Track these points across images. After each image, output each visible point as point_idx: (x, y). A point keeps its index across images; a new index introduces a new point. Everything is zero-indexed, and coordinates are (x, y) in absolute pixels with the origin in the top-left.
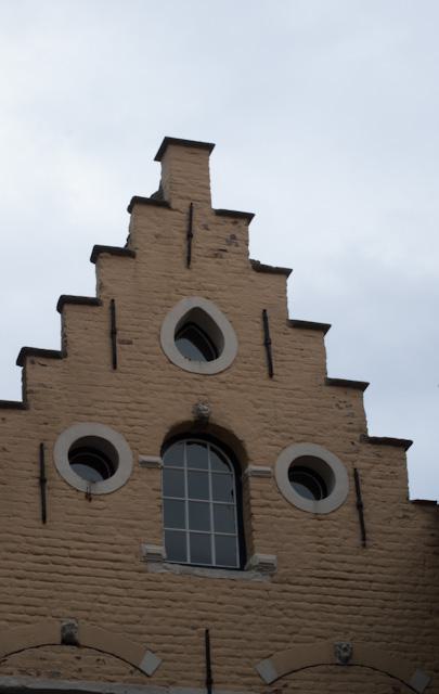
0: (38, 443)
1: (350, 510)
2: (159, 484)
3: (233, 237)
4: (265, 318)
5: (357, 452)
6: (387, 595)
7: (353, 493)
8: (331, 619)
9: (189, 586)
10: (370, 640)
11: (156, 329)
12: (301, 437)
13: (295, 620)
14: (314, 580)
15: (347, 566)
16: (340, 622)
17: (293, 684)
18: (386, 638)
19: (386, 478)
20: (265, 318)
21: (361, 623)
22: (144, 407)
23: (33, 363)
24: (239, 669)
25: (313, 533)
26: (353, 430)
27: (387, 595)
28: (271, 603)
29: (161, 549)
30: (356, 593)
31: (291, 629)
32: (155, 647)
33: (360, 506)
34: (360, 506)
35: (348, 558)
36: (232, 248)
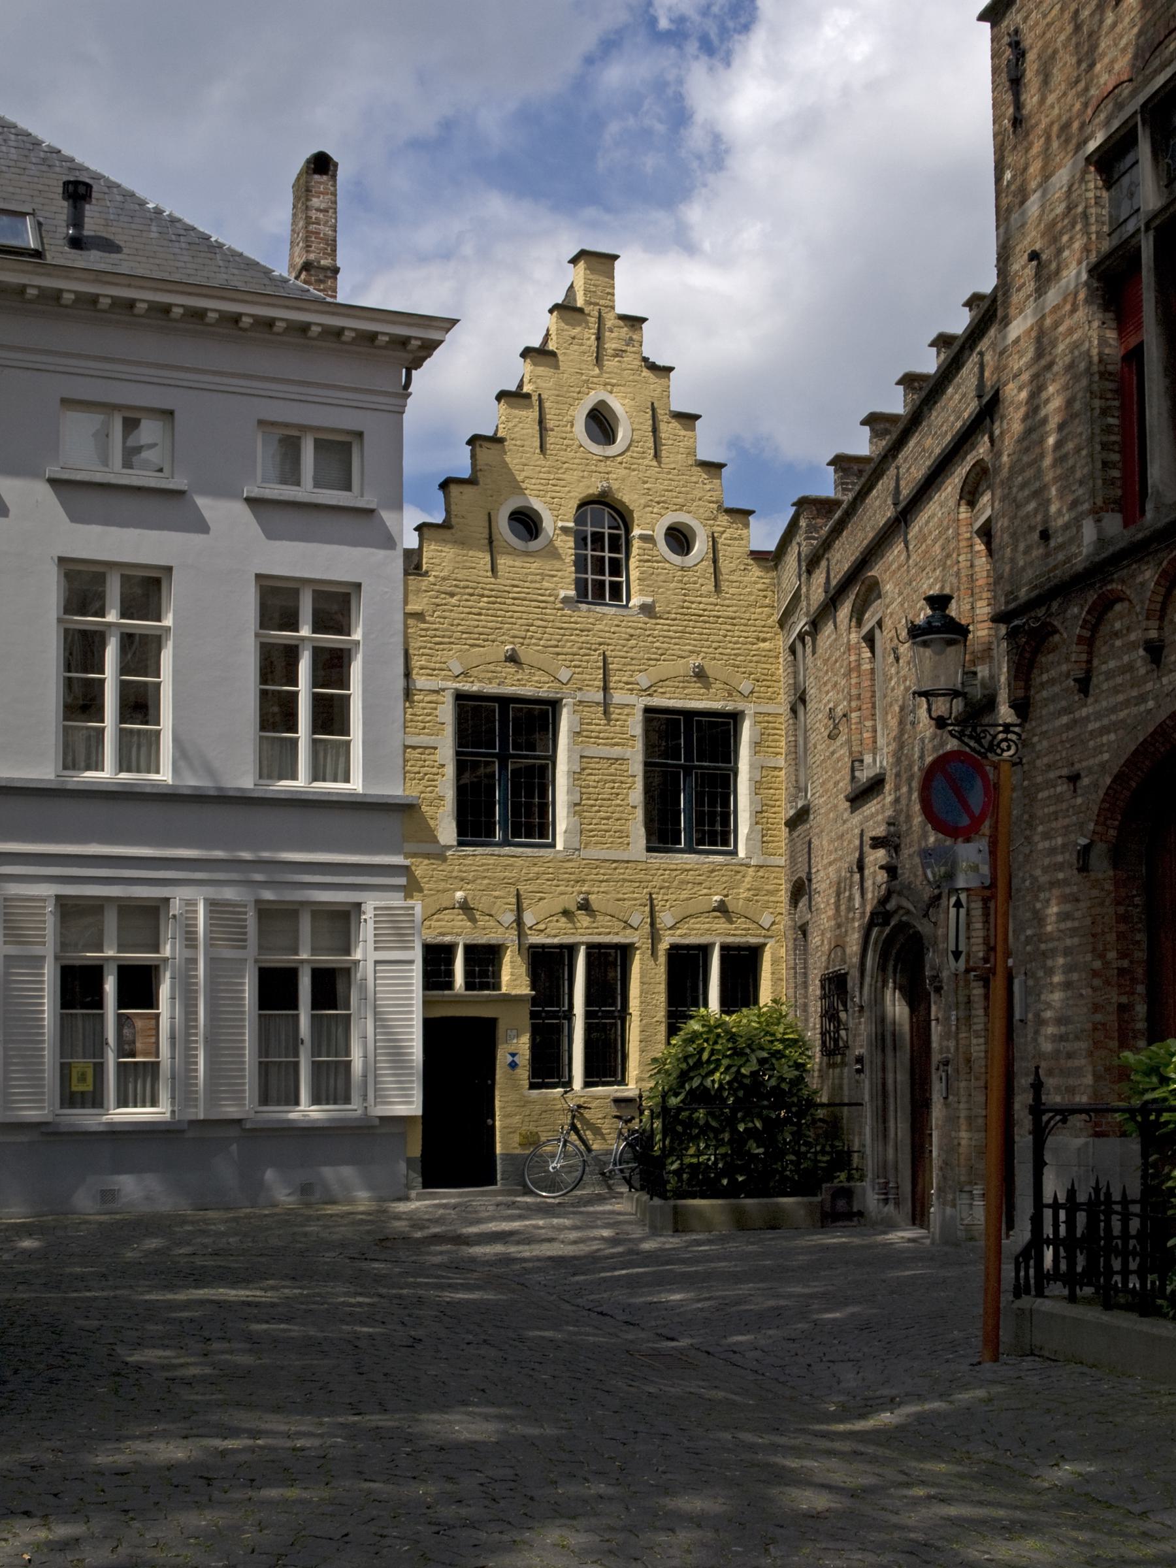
0: (119, 240)
1: (707, 564)
2: (572, 544)
3: (631, 339)
4: (653, 409)
5: (715, 519)
6: (729, 627)
7: (711, 551)
8: (689, 644)
9: (590, 620)
10: (715, 659)
11: (570, 418)
12: (675, 507)
13: (665, 645)
14: (679, 616)
15: (701, 606)
16: (695, 646)
17: (660, 690)
18: (725, 657)
19: (735, 539)
20: (653, 409)
21: (709, 647)
22: (562, 483)
23: (481, 446)
24: (624, 679)
25: (681, 581)
26: (712, 502)
27: (729, 627)
28: (648, 633)
29: (572, 593)
30: (707, 625)
31: (660, 652)
32: (568, 663)
33: (715, 561)
34: (715, 561)
35: (704, 600)
36: (629, 349)
